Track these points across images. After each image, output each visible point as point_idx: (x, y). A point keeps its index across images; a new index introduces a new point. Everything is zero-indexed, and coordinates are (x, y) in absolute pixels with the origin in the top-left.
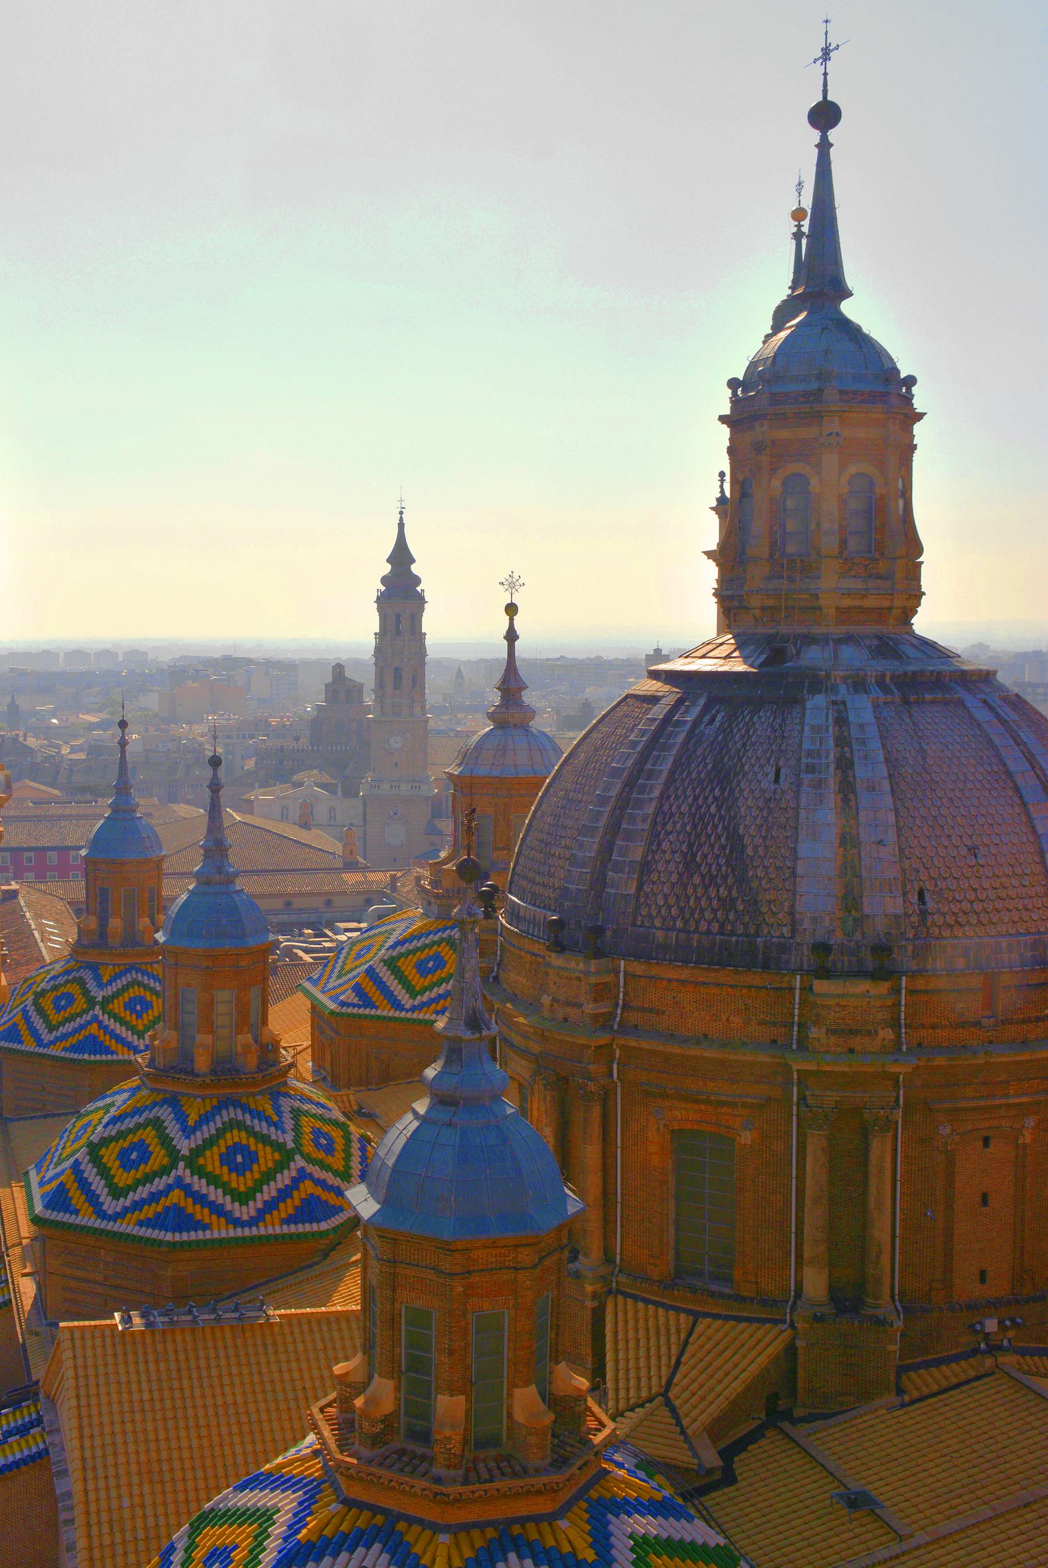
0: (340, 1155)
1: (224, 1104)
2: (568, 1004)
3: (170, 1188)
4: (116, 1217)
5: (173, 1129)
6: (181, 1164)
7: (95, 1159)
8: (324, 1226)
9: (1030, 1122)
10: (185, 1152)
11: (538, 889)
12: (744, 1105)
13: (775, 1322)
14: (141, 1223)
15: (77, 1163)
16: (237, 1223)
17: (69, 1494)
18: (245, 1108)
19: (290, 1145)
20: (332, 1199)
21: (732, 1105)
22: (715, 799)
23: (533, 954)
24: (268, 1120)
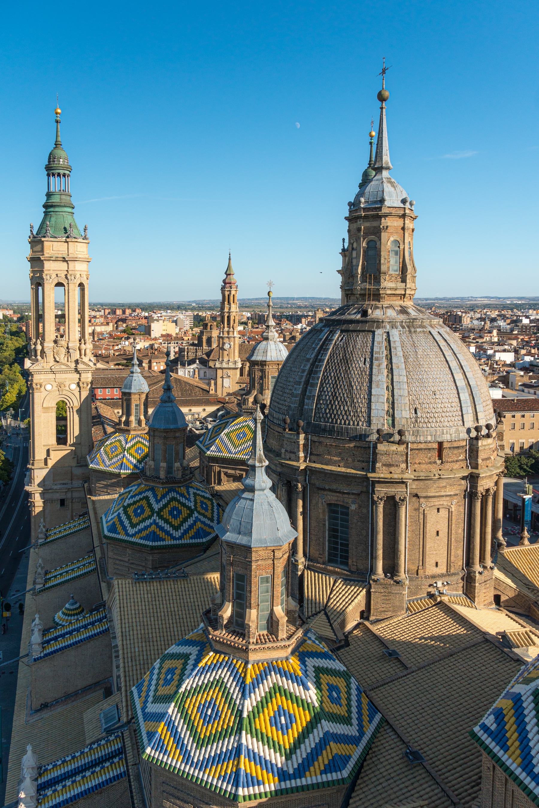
0: (210, 511)
1: (170, 490)
2: (291, 452)
3: (151, 524)
4: (133, 535)
5: (152, 500)
6: (155, 515)
7: (126, 512)
8: (204, 540)
9: (455, 501)
10: (156, 510)
11: (280, 406)
12: (353, 494)
13: (363, 582)
14: (141, 538)
15: (119, 514)
16: (174, 538)
17: (116, 646)
18: (178, 493)
19: (193, 507)
20: (208, 529)
21: (348, 494)
22: (343, 371)
23: (279, 432)
24: (185, 497)
